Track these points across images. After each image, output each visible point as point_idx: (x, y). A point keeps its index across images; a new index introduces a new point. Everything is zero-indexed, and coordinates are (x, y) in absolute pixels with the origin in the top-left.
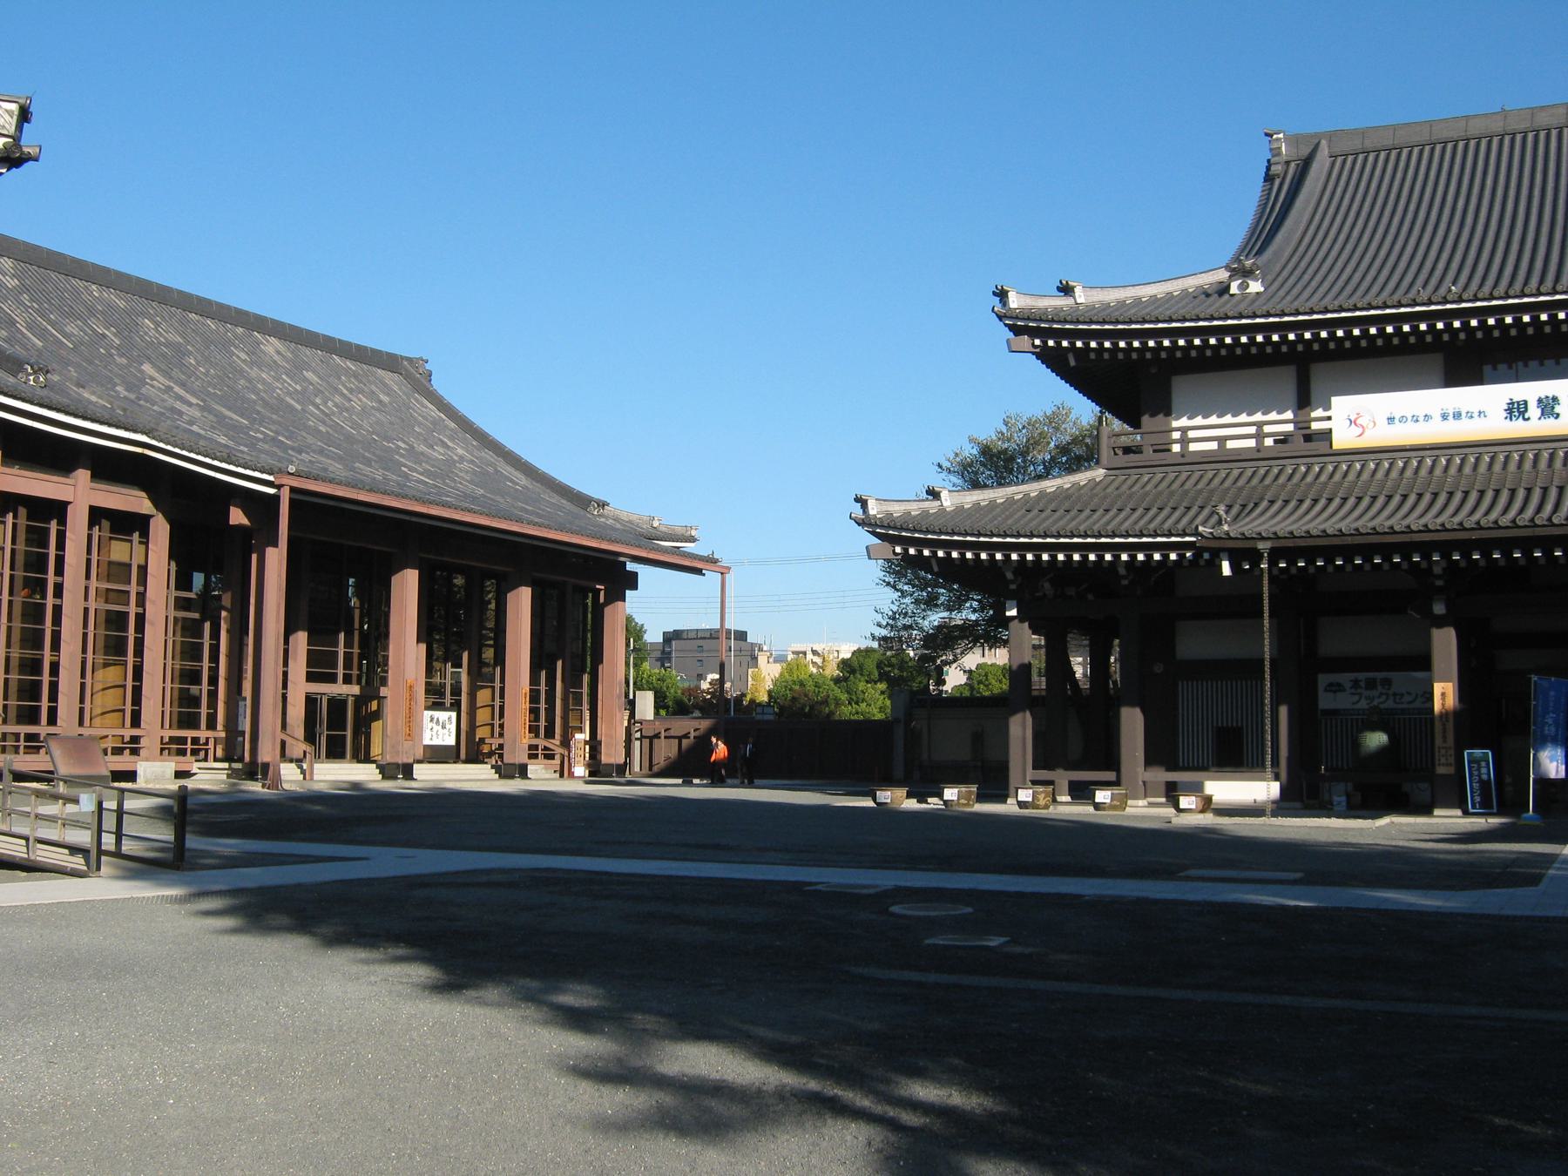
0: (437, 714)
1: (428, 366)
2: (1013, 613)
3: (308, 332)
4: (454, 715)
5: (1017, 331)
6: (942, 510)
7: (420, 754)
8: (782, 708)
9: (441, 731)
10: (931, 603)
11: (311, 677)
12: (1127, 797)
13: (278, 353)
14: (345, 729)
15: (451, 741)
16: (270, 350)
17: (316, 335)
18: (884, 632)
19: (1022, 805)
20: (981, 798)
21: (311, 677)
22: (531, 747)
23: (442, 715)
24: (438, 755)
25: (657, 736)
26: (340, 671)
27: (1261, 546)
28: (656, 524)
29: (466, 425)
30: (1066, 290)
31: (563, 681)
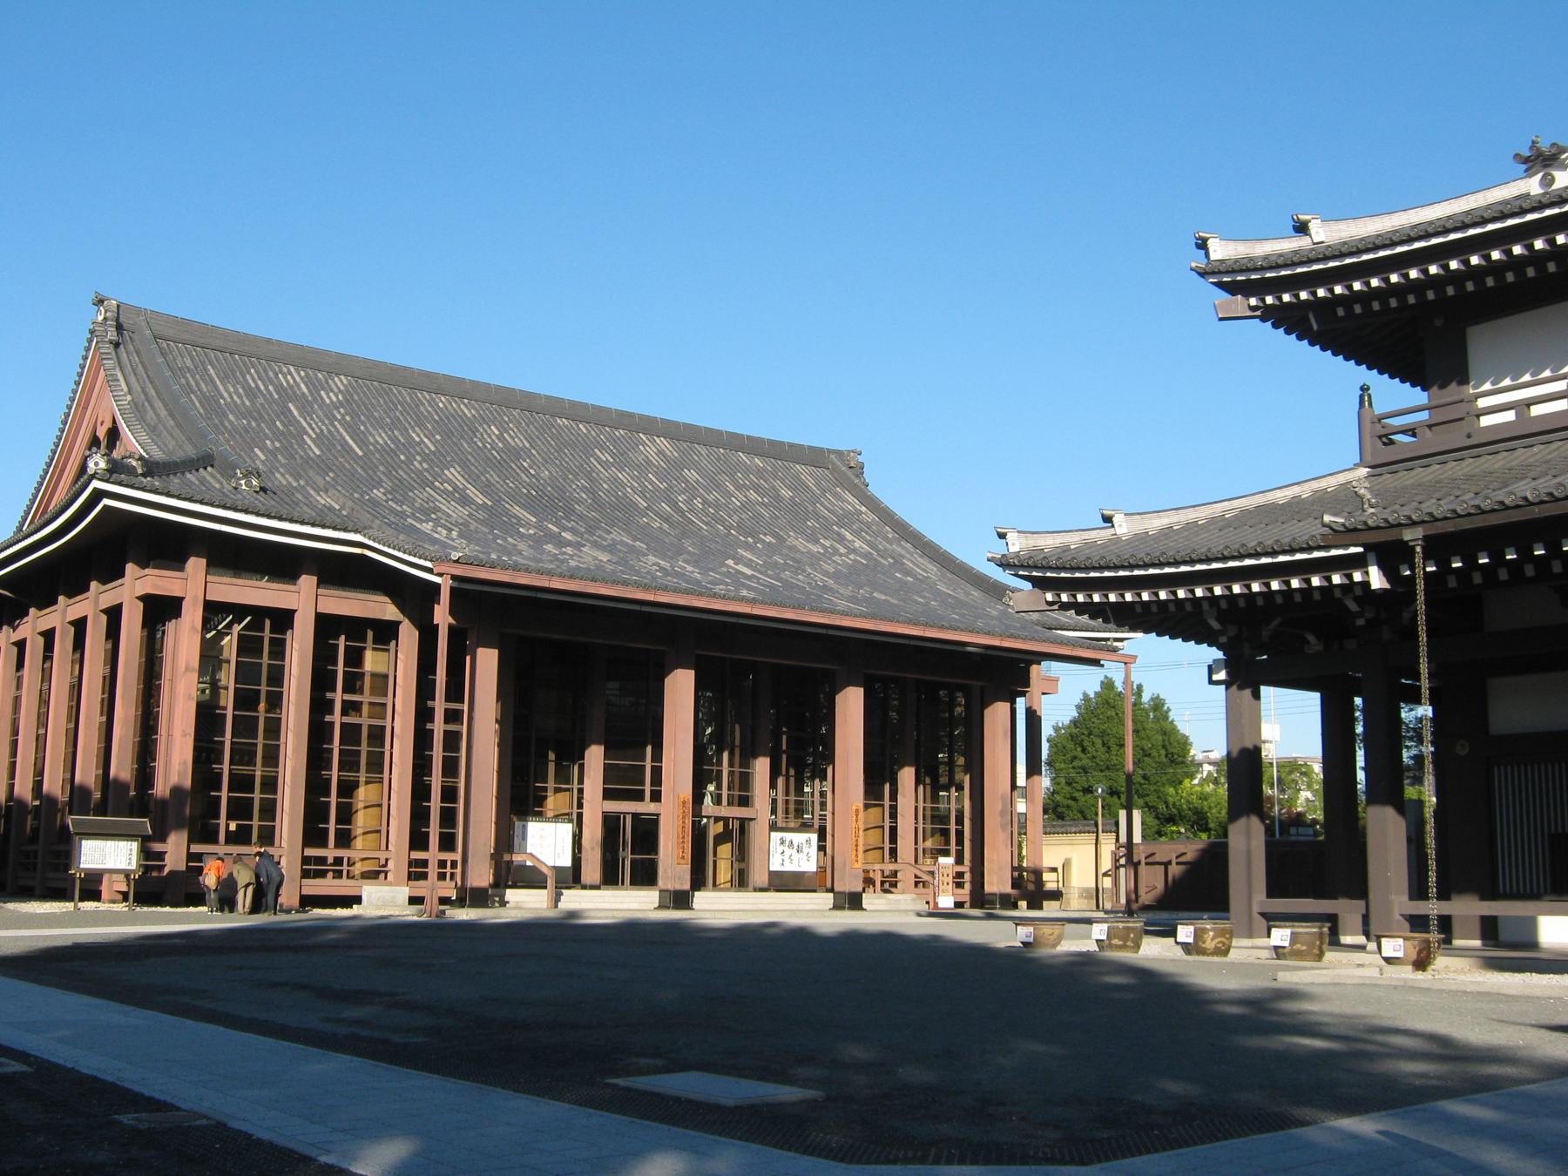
0: (788, 836)
1: (860, 458)
4: (814, 837)
5: (1232, 288)
6: (1116, 540)
11: (608, 795)
12: (1232, 934)
13: (660, 452)
16: (651, 451)
21: (608, 795)
23: (799, 838)
26: (648, 788)
27: (1408, 535)
30: (1302, 228)
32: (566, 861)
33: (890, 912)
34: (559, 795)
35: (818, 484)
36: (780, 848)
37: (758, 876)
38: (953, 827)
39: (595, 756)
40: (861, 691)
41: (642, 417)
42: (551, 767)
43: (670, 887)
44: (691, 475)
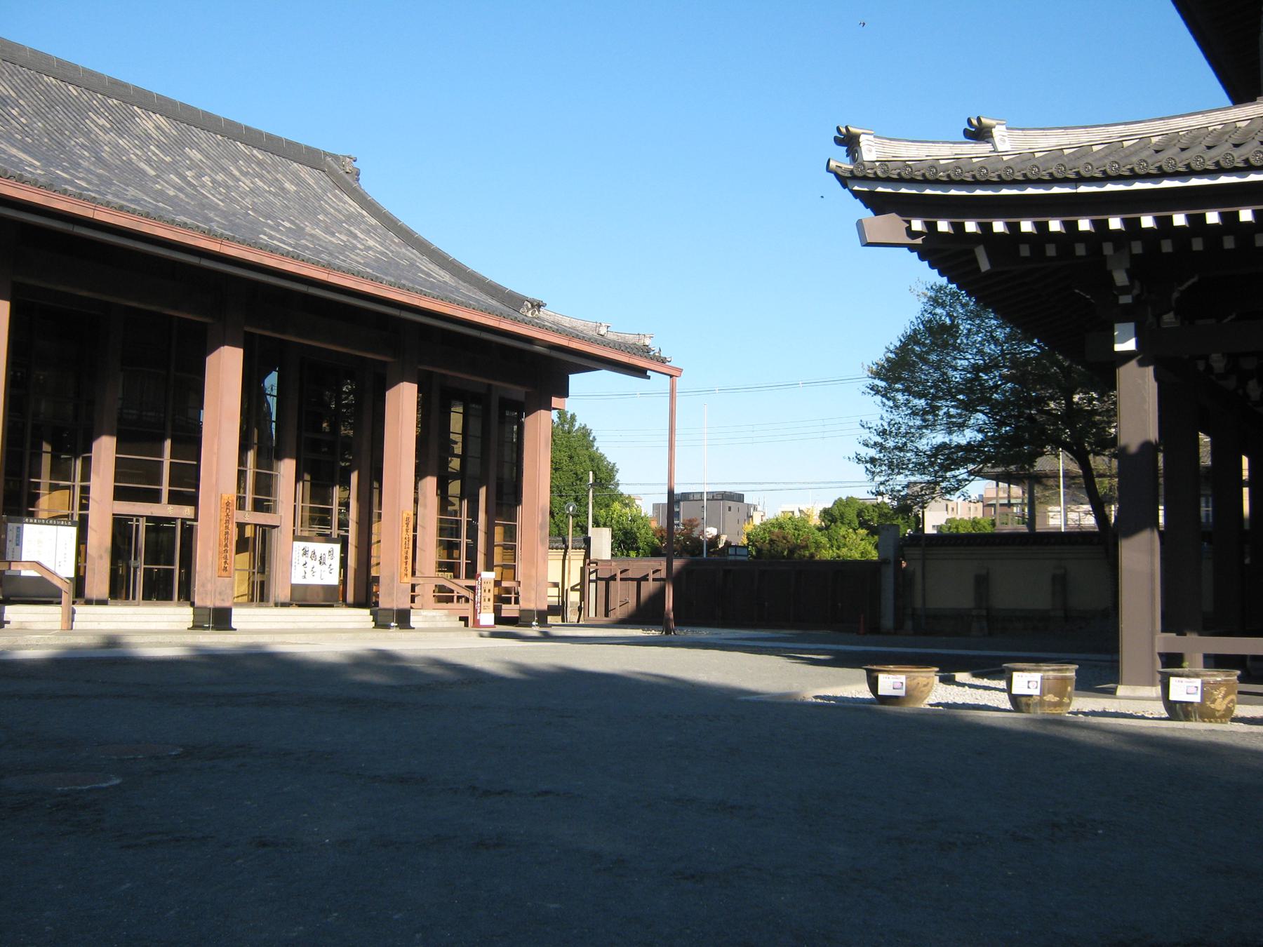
0: (311, 546)
2: (1130, 345)
4: (337, 548)
7: (283, 593)
8: (759, 551)
10: (928, 417)
11: (121, 494)
13: (158, 128)
14: (172, 564)
15: (334, 579)
16: (150, 126)
17: (218, 119)
18: (873, 453)
19: (1177, 710)
20: (1086, 684)
21: (121, 494)
22: (441, 588)
23: (321, 548)
24: (305, 598)
25: (613, 578)
26: (165, 488)
29: (390, 223)
31: (487, 512)
33: (441, 636)
34: (57, 494)
35: (317, 183)
36: (303, 560)
37: (280, 591)
38: (464, 540)
39: (105, 450)
41: (136, 89)
42: (46, 460)
43: (210, 604)
44: (195, 155)
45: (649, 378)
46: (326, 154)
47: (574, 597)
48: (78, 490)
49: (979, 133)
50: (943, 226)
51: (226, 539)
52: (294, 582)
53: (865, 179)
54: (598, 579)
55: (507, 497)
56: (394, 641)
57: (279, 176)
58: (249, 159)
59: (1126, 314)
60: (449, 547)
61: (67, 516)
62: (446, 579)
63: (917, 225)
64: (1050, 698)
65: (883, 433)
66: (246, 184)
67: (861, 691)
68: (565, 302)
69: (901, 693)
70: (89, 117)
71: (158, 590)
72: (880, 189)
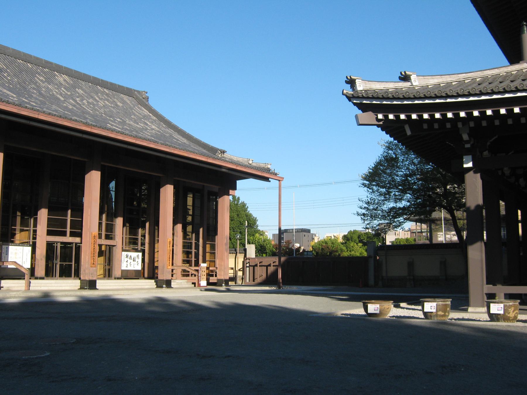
0: (130, 254)
2: (470, 165)
3: (85, 74)
4: (140, 254)
8: (317, 253)
9: (132, 263)
10: (387, 196)
13: (65, 80)
14: (72, 262)
15: (139, 267)
16: (61, 80)
18: (364, 211)
19: (494, 317)
20: (455, 307)
22: (184, 271)
23: (134, 254)
24: (127, 275)
25: (256, 265)
26: (68, 230)
28: (251, 162)
29: (161, 119)
31: (203, 239)
32: (28, 265)
33: (184, 290)
34: (23, 233)
35: (131, 103)
36: (126, 259)
37: (117, 273)
38: (193, 250)
39: (43, 214)
40: (172, 187)
42: (19, 219)
43: (87, 278)
45: (270, 181)
46: (135, 90)
47: (240, 274)
48: (32, 231)
49: (405, 78)
50: (391, 117)
51: (94, 251)
52: (122, 269)
53: (358, 98)
54: (250, 266)
55: (212, 232)
56: (165, 293)
57: (115, 100)
58: (103, 93)
59: (468, 152)
60: (187, 253)
61: (27, 242)
62: (186, 267)
63: (380, 116)
64: (440, 313)
65: (368, 203)
66: (101, 103)
67: (361, 311)
68: (235, 150)
69: (378, 312)
70: (36, 76)
71: (65, 273)
72: (364, 102)
